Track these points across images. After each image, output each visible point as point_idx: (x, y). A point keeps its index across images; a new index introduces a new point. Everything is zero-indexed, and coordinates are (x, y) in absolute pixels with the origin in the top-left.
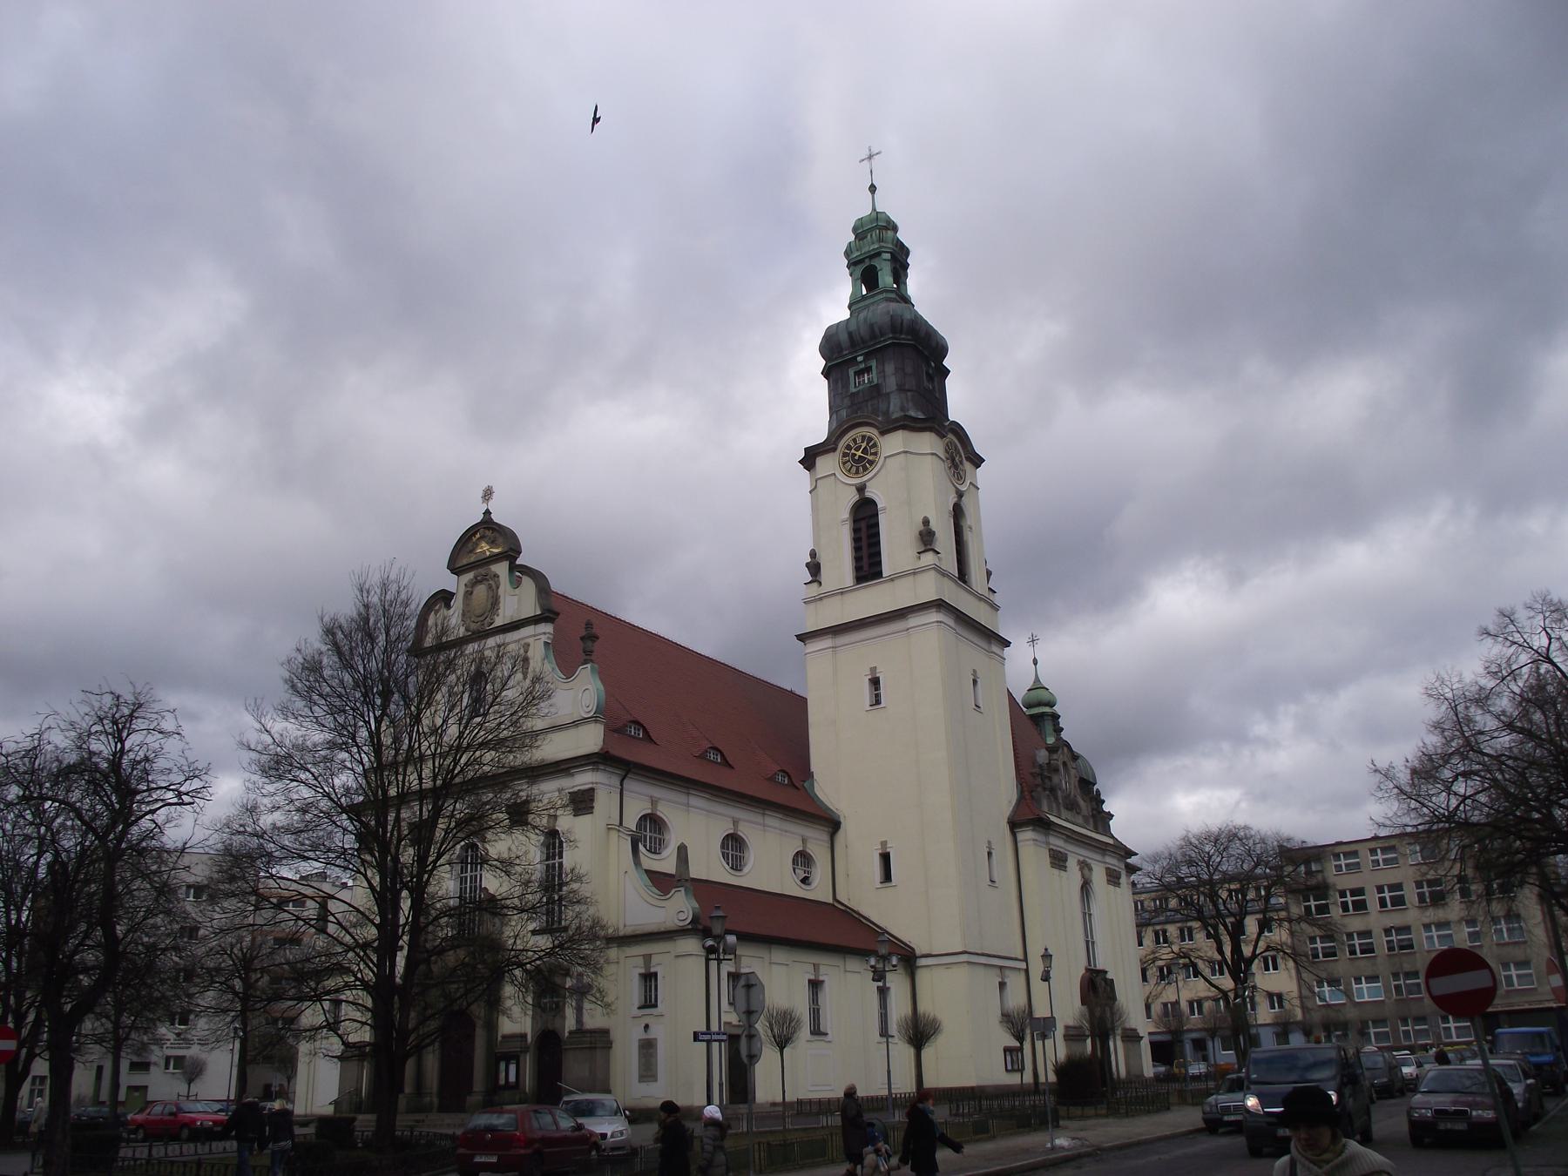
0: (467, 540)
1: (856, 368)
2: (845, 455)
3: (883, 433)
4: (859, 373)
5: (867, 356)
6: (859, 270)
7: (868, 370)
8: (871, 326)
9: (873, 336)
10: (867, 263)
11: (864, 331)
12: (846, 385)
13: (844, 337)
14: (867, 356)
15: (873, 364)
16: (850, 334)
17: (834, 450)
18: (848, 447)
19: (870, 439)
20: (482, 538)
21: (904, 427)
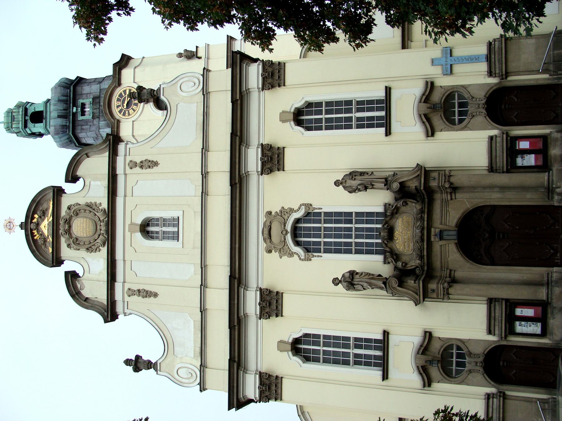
0: (35, 246)
1: (79, 114)
2: (124, 115)
3: (120, 84)
4: (83, 113)
5: (75, 105)
6: (30, 124)
7: (83, 105)
8: (59, 101)
9: (66, 102)
10: (28, 118)
11: (61, 106)
12: (86, 122)
13: (60, 121)
14: (75, 105)
15: (81, 101)
16: (59, 117)
17: (119, 121)
18: (120, 112)
19: (121, 95)
20: (38, 224)
21: (120, 69)
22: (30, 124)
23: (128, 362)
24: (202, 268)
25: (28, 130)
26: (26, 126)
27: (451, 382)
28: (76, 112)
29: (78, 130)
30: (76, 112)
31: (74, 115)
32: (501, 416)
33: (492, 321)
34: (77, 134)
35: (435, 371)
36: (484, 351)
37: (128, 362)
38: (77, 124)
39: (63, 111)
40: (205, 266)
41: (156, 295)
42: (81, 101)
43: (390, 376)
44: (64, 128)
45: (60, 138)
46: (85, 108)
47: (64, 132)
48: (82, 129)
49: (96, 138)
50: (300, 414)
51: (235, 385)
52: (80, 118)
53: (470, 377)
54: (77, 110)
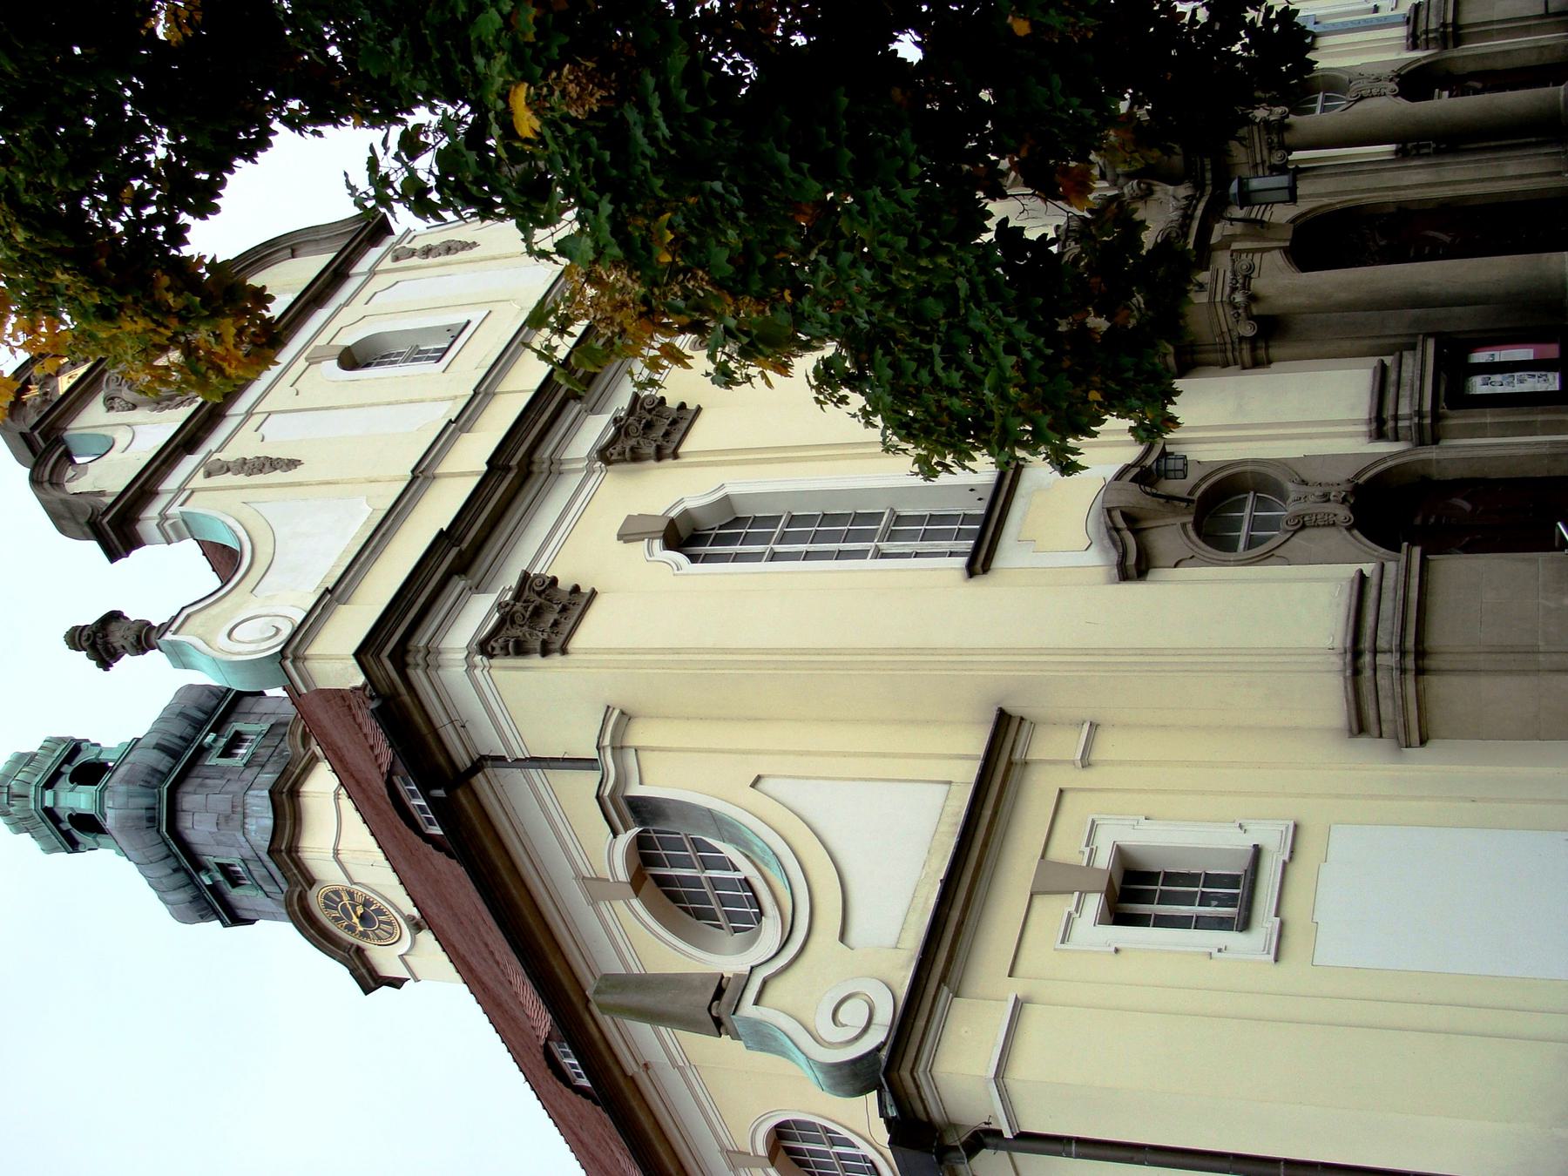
5: (217, 728)
7: (238, 739)
8: (183, 715)
10: (68, 769)
22: (64, 784)
23: (78, 638)
24: (476, 392)
25: (49, 794)
26: (50, 784)
27: (1224, 563)
28: (211, 747)
29: (189, 786)
30: (211, 747)
31: (202, 751)
32: (1414, 595)
33: (1391, 391)
34: (179, 796)
35: (1169, 536)
36: (1357, 476)
37: (78, 638)
38: (195, 772)
39: (177, 741)
40: (486, 394)
41: (293, 464)
42: (237, 726)
43: (999, 561)
44: (158, 775)
45: (130, 795)
46: (239, 747)
47: (147, 785)
48: (201, 785)
49: (227, 818)
50: (607, 741)
51: (422, 600)
52: (213, 760)
53: (1298, 540)
54: (215, 740)
